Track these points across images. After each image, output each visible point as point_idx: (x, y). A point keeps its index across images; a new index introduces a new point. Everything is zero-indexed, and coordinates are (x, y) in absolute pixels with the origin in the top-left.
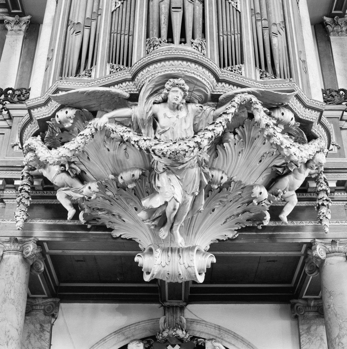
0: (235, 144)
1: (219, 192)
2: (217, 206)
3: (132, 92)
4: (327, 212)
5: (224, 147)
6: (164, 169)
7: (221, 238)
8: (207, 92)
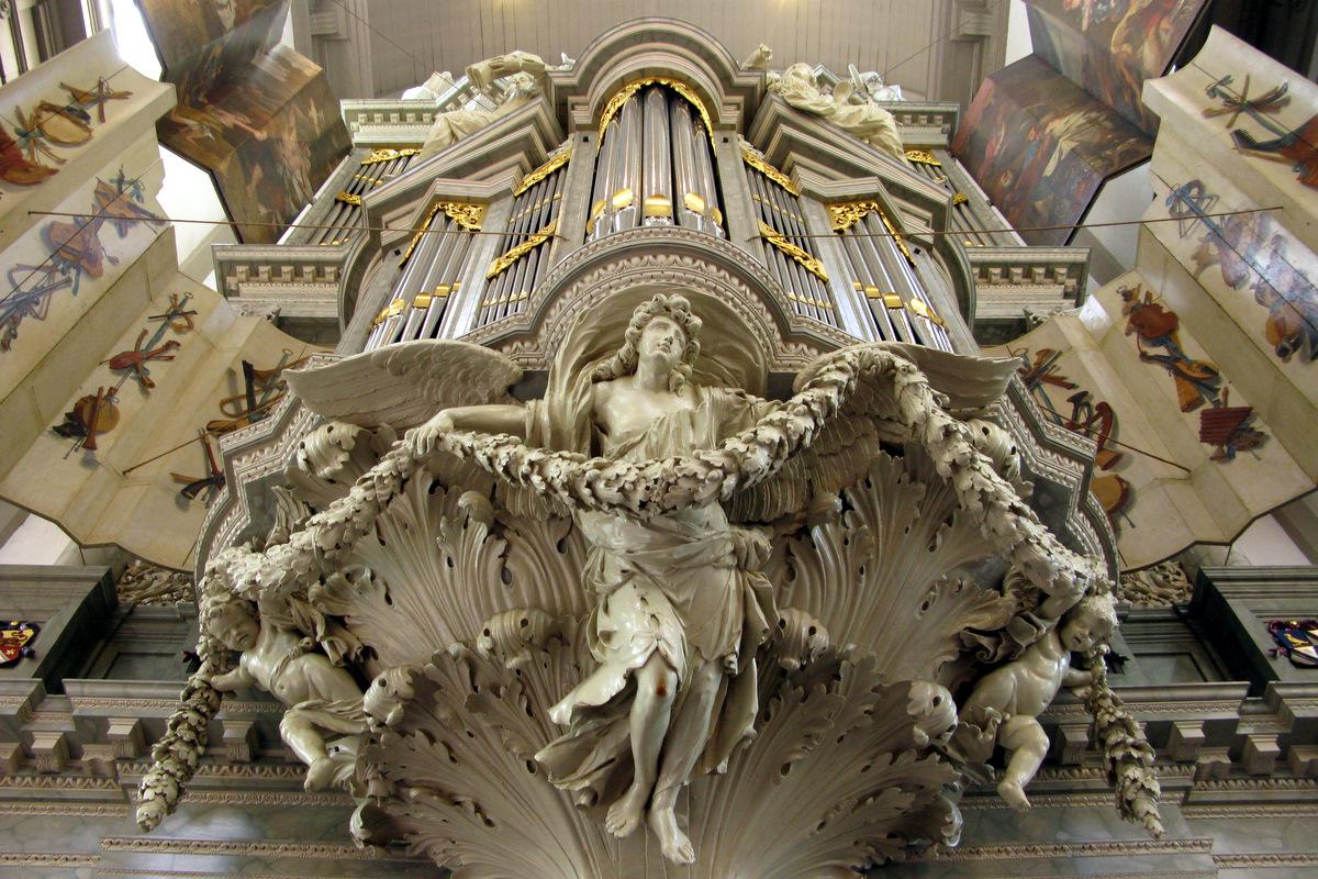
0: (846, 542)
1: (804, 699)
2: (798, 756)
3: (530, 369)
4: (1146, 775)
5: (814, 547)
6: (624, 571)
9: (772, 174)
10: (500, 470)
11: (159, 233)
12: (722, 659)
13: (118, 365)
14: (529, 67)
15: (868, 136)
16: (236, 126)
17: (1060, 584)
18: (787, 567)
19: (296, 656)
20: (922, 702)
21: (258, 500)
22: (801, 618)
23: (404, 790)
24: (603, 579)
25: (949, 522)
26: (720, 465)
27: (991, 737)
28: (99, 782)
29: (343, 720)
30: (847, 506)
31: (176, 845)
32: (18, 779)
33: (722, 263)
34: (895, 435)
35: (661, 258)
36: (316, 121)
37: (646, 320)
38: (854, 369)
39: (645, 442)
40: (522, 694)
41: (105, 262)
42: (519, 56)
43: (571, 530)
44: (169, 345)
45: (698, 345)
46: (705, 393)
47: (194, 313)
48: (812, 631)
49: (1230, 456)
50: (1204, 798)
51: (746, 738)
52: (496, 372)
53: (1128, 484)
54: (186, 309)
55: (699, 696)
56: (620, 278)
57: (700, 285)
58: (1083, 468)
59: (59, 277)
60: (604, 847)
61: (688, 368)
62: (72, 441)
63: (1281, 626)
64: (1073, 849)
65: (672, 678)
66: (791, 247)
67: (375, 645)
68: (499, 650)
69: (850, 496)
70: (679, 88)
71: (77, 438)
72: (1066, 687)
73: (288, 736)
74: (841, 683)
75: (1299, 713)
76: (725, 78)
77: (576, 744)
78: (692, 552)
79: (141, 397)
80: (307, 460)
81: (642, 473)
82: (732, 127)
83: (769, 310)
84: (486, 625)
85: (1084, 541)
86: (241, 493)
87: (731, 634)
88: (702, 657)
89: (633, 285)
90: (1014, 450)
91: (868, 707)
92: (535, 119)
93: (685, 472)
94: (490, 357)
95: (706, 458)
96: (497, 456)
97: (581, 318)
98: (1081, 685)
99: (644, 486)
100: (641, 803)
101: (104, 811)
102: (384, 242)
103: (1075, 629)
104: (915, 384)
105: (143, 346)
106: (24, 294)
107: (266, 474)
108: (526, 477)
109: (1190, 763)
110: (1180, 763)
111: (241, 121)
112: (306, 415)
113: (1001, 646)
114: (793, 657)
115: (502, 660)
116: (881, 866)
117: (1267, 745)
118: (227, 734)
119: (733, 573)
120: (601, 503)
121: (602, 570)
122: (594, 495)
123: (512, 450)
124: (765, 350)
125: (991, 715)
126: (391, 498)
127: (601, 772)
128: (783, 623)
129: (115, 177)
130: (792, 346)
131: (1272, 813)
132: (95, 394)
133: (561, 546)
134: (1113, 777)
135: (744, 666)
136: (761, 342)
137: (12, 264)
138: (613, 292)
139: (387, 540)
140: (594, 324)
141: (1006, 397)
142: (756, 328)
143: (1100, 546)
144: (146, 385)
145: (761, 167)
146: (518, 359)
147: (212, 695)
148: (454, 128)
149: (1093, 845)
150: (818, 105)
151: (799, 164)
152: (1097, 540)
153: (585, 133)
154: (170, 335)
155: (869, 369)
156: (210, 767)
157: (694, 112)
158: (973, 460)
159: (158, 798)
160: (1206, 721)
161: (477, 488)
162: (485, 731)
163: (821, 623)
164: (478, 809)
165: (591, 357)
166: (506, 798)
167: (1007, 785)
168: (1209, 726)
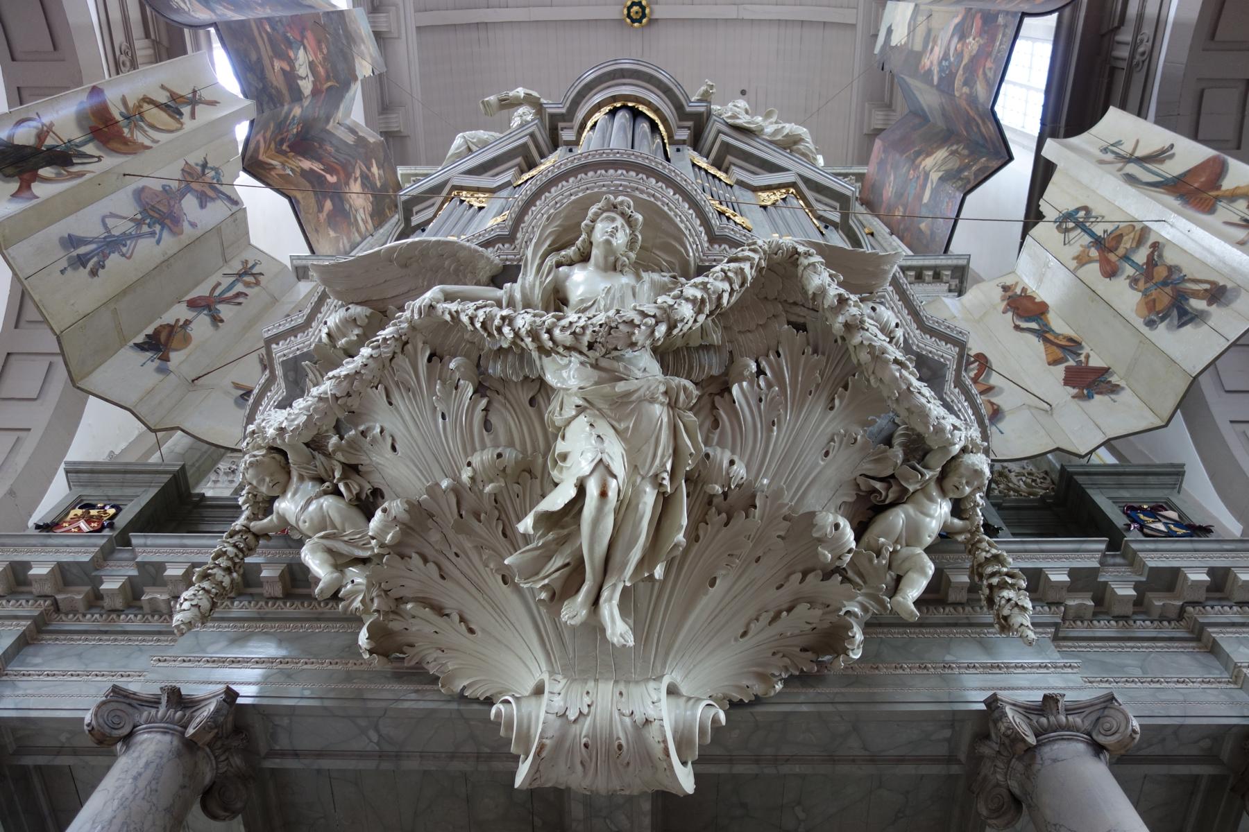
1: (726, 525)
3: (508, 263)
4: (1018, 596)
5: (734, 402)
6: (577, 406)
7: (737, 696)
8: (688, 255)
9: (713, 171)
10: (478, 325)
11: (233, 211)
12: (656, 476)
13: (192, 304)
14: (529, 100)
15: (789, 148)
16: (311, 169)
17: (939, 430)
18: (713, 419)
19: (318, 497)
20: (823, 527)
21: (291, 375)
22: (722, 453)
23: (402, 606)
24: (561, 415)
25: (846, 387)
26: (652, 314)
27: (884, 562)
28: (156, 617)
30: (760, 372)
31: (214, 661)
32: (89, 616)
33: (660, 177)
34: (799, 316)
35: (611, 172)
36: (377, 176)
37: (597, 215)
38: (765, 252)
39: (596, 306)
41: (186, 225)
42: (521, 92)
43: (539, 391)
44: (238, 295)
45: (640, 237)
46: (645, 276)
48: (732, 463)
49: (1090, 397)
50: (1072, 634)
51: (677, 546)
52: (482, 264)
53: (998, 406)
54: (255, 271)
55: (637, 505)
56: (578, 187)
57: (642, 192)
58: (957, 349)
59: (145, 229)
60: (560, 636)
62: (149, 354)
63: (1132, 508)
65: (613, 484)
66: (724, 208)
68: (479, 479)
69: (764, 364)
70: (642, 108)
71: (155, 352)
72: (946, 535)
73: (307, 558)
74: (757, 510)
76: (679, 107)
77: (538, 552)
78: (632, 388)
79: (211, 328)
80: (329, 334)
81: (589, 322)
82: (684, 142)
83: (697, 216)
84: (469, 460)
85: (960, 410)
86: (279, 372)
87: (663, 456)
89: (588, 192)
90: (897, 325)
91: (782, 533)
92: (532, 135)
93: (624, 319)
94: (477, 251)
95: (641, 309)
96: (476, 316)
97: (548, 219)
98: (960, 532)
100: (592, 598)
101: (158, 640)
102: (413, 224)
103: (952, 480)
104: (813, 264)
105: (217, 293)
106: (114, 236)
107: (298, 353)
108: (499, 329)
109: (1058, 604)
110: (1050, 604)
111: (317, 167)
112: (332, 301)
114: (716, 483)
115: (481, 488)
118: (265, 573)
119: (666, 408)
120: (557, 346)
121: (561, 409)
122: (551, 339)
123: (488, 309)
124: (695, 246)
125: (883, 544)
126: (393, 357)
127: (557, 574)
128: (707, 456)
129: (201, 163)
130: (716, 246)
131: (1132, 647)
132: (172, 322)
133: (532, 402)
134: (991, 601)
135: (676, 490)
136: (691, 240)
137: (106, 212)
138: (573, 198)
139: (394, 402)
140: (558, 223)
141: (891, 288)
142: (687, 228)
143: (973, 417)
144: (216, 320)
145: (704, 165)
146: (499, 256)
147: (250, 537)
149: (977, 665)
150: (749, 123)
151: (734, 165)
152: (970, 412)
153: (570, 147)
154: (239, 287)
155: (776, 254)
156: (250, 602)
157: (654, 127)
158: (862, 322)
159: (193, 609)
160: (1071, 569)
161: (467, 356)
162: (468, 551)
163: (741, 458)
164: (462, 619)
165: (556, 248)
166: (484, 608)
167: (899, 598)
168: (1073, 572)
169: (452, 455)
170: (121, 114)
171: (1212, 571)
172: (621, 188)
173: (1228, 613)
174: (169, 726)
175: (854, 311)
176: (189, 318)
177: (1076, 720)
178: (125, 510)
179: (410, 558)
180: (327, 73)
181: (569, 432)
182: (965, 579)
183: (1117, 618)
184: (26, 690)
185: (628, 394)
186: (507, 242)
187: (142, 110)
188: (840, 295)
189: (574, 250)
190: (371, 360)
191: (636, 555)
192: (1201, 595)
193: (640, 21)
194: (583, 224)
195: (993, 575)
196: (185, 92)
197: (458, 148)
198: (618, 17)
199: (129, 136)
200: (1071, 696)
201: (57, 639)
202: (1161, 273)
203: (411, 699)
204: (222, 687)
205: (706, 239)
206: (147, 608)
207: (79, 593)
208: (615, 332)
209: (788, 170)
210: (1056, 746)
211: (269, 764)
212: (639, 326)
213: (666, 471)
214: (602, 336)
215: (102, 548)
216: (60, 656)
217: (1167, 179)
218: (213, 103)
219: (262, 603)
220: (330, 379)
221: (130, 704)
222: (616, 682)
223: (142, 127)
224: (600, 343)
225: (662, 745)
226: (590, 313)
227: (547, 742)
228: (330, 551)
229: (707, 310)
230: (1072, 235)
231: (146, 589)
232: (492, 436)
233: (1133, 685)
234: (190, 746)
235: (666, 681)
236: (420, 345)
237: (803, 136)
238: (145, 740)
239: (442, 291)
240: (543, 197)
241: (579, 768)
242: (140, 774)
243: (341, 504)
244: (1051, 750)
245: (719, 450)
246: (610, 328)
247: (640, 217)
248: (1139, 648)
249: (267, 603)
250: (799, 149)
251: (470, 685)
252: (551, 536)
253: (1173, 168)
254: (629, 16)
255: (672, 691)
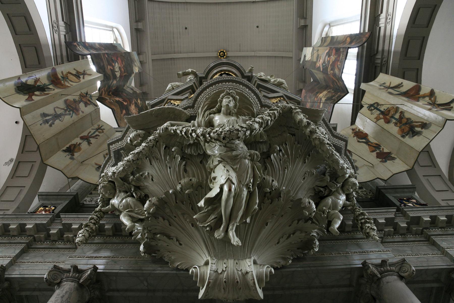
1: (271, 203)
2: (270, 220)
3: (192, 115)
6: (218, 161)
8: (254, 111)
10: (183, 133)
11: (96, 108)
12: (247, 185)
13: (82, 138)
15: (279, 86)
16: (119, 100)
17: (343, 168)
19: (126, 198)
20: (305, 203)
22: (269, 178)
23: (156, 236)
25: (309, 156)
26: (245, 127)
28: (68, 243)
29: (138, 214)
31: (89, 257)
32: (45, 243)
36: (140, 103)
37: (223, 97)
38: (281, 108)
39: (224, 126)
40: (190, 204)
41: (80, 112)
42: (190, 70)
43: (203, 158)
44: (97, 135)
46: (241, 117)
47: (104, 129)
50: (387, 241)
51: (255, 210)
54: (102, 128)
55: (241, 195)
57: (238, 89)
58: (345, 143)
59: (67, 112)
60: (213, 245)
61: (235, 110)
62: (67, 153)
63: (400, 199)
64: (351, 253)
65: (233, 187)
67: (148, 194)
68: (183, 189)
69: (281, 148)
72: (344, 206)
73: (122, 219)
75: (411, 215)
77: (205, 214)
78: (238, 153)
79: (88, 146)
80: (130, 140)
86: (112, 155)
87: (250, 178)
88: (242, 184)
89: (220, 90)
91: (290, 206)
96: (183, 130)
97: (206, 99)
98: (349, 206)
99: (224, 132)
101: (69, 251)
104: (298, 112)
105: (90, 135)
106: (58, 114)
107: (119, 148)
108: (191, 134)
109: (382, 230)
111: (121, 100)
112: (131, 129)
113: (326, 191)
116: (296, 258)
117: (404, 225)
119: (250, 161)
121: (213, 162)
122: (210, 136)
123: (187, 128)
125: (325, 209)
127: (213, 221)
128: (264, 178)
130: (263, 108)
131: (407, 244)
132: (75, 144)
133: (201, 162)
134: (362, 228)
135: (254, 190)
136: (255, 106)
137: (55, 106)
141: (322, 122)
142: (253, 102)
144: (89, 143)
146: (189, 113)
147: (102, 213)
148: (173, 87)
149: (357, 252)
150: (265, 78)
154: (97, 133)
155: (285, 109)
156: (101, 237)
158: (316, 130)
164: (177, 240)
168: (386, 219)
169: (173, 181)
170: (61, 77)
171: (431, 217)
172: (231, 88)
173: (437, 231)
174: (74, 279)
175: (313, 127)
176: (81, 142)
177: (393, 268)
178: (58, 208)
179: (159, 218)
180: (124, 70)
181: (216, 170)
182: (351, 223)
183: (401, 235)
184: (23, 268)
185: (237, 156)
186: (192, 108)
187: (68, 76)
188: (307, 122)
189: (215, 109)
190: (145, 147)
191: (241, 213)
192: (428, 225)
193: (223, 57)
194: (218, 100)
195: (362, 219)
196: (82, 71)
197: (169, 88)
198: (216, 56)
199: (63, 83)
200: (390, 261)
201: (34, 251)
202: (404, 121)
203: (159, 270)
204: (92, 266)
205: (260, 106)
206: (65, 240)
207: (42, 234)
208: (233, 133)
209: (280, 92)
210: (387, 278)
211: (108, 294)
212: (241, 131)
213: (251, 183)
214: (228, 135)
215: (51, 218)
216: (35, 257)
217: (402, 93)
218: (90, 75)
219: (105, 238)
220: (131, 154)
221: (60, 272)
222: (234, 260)
223: (67, 81)
224: (227, 137)
225: (253, 281)
226: (223, 128)
227: (211, 281)
228: (130, 216)
229: (263, 126)
230: (374, 111)
231: (65, 233)
232: (187, 175)
233: (409, 257)
234: (81, 286)
235: (253, 258)
236: (162, 143)
237: (284, 82)
238: (65, 284)
239: (170, 123)
240: (204, 92)
241: (222, 290)
242: (64, 296)
243: (134, 200)
244: (386, 279)
245: (268, 177)
246: (230, 131)
247: (238, 97)
248: (409, 244)
249: (107, 238)
250: (283, 86)
251: (180, 264)
252: (210, 208)
253: (403, 89)
254: (220, 55)
255: (255, 263)
